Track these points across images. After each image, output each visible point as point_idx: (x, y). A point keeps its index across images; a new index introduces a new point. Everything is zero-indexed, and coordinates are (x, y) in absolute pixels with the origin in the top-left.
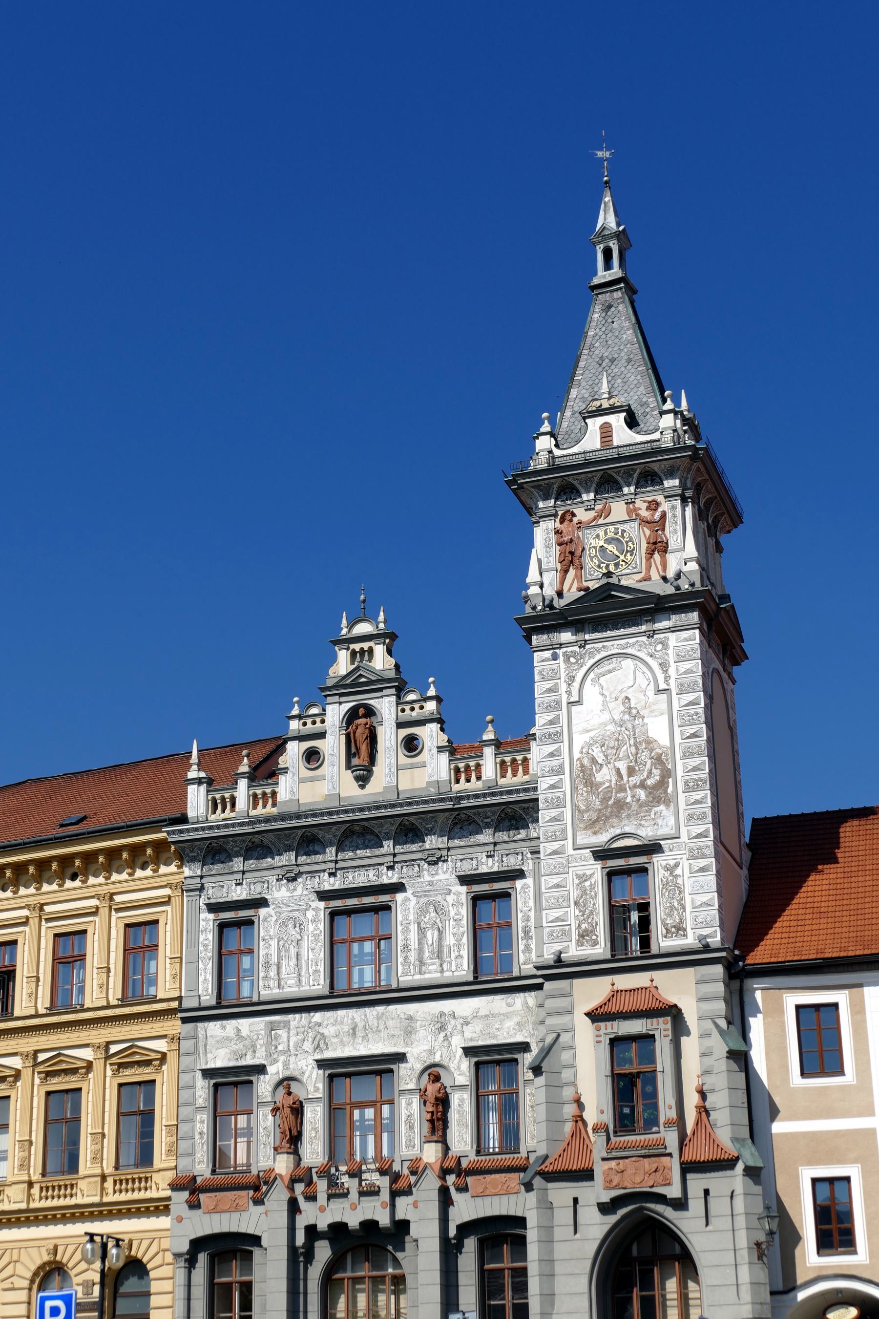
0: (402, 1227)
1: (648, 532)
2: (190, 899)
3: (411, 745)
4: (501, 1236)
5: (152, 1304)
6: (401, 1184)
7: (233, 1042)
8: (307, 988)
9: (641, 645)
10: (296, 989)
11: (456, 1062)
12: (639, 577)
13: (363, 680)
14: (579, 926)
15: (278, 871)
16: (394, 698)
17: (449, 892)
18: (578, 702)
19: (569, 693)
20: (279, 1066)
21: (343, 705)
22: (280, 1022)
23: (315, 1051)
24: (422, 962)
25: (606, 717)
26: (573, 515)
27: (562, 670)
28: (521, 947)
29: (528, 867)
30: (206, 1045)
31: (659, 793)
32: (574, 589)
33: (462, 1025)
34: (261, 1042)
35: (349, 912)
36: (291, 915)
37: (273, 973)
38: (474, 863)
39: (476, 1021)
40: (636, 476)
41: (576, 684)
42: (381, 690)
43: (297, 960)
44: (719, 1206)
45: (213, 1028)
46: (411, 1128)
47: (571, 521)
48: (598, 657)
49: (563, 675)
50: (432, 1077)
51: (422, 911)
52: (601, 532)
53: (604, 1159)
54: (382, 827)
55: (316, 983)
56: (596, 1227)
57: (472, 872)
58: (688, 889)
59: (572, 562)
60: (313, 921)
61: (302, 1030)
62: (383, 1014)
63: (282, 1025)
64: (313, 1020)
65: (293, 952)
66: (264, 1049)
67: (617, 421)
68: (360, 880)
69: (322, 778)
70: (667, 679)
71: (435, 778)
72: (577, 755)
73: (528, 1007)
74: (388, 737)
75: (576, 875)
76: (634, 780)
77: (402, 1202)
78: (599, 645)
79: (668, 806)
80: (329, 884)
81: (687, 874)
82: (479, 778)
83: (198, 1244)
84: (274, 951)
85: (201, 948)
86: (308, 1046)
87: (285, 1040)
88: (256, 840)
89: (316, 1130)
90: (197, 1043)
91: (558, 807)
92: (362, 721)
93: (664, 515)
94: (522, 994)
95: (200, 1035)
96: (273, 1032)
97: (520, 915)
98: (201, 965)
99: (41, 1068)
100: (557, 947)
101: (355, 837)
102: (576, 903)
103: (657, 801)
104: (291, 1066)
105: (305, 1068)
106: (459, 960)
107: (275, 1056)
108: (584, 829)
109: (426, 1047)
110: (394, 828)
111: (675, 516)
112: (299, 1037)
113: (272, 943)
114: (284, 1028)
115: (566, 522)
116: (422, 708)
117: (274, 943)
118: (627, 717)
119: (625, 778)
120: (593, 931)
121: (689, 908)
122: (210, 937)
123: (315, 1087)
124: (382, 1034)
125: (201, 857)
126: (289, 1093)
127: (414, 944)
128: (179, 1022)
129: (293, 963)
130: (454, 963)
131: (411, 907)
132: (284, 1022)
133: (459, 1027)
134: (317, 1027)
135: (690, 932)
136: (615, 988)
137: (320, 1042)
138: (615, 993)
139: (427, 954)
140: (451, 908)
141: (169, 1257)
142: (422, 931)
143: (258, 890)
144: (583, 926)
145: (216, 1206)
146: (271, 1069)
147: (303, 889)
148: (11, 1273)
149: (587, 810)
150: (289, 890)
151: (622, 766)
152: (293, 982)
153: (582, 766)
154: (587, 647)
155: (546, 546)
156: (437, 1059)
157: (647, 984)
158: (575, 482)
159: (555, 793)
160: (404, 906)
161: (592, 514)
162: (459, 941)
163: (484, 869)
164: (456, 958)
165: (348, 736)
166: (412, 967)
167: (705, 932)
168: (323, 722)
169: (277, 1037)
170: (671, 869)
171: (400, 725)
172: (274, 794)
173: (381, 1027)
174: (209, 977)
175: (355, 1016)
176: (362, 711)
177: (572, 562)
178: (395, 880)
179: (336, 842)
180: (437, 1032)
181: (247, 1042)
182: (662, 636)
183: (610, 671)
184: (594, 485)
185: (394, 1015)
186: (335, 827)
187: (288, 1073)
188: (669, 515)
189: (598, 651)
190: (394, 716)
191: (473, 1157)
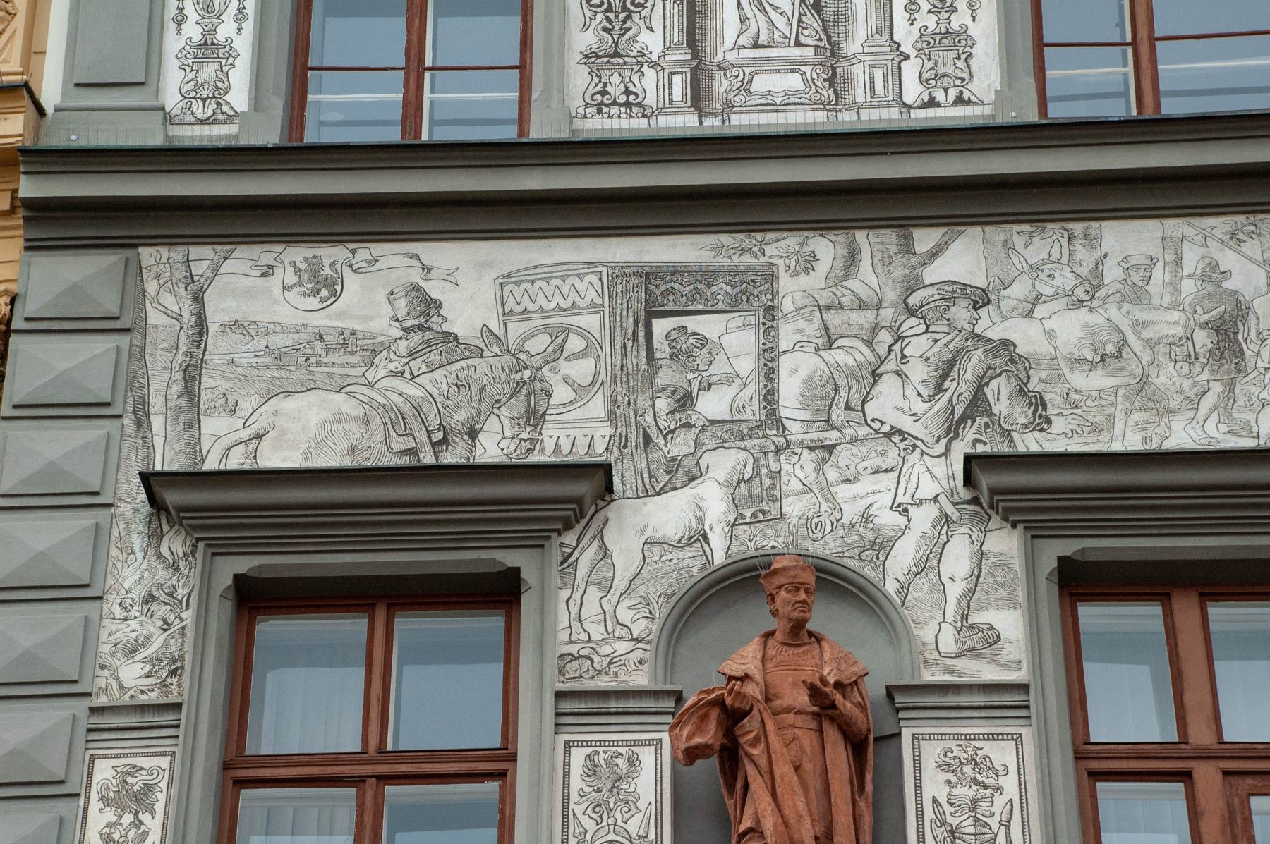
20: (710, 500)
22: (709, 276)
23: (953, 430)
30: (191, 373)
34: (582, 370)
45: (256, 289)
61: (863, 319)
63: (722, 288)
64: (933, 274)
66: (597, 406)
87: (746, 365)
95: (154, 317)
96: (661, 327)
104: (794, 508)
105: (887, 519)
107: (680, 446)
112: (837, 356)
114: (733, 306)
123: (964, 623)
126: (799, 633)
132: (735, 275)
134: (961, 313)
152: (794, 82)
175: (1228, 259)
181: (480, 370)
187: (768, 539)
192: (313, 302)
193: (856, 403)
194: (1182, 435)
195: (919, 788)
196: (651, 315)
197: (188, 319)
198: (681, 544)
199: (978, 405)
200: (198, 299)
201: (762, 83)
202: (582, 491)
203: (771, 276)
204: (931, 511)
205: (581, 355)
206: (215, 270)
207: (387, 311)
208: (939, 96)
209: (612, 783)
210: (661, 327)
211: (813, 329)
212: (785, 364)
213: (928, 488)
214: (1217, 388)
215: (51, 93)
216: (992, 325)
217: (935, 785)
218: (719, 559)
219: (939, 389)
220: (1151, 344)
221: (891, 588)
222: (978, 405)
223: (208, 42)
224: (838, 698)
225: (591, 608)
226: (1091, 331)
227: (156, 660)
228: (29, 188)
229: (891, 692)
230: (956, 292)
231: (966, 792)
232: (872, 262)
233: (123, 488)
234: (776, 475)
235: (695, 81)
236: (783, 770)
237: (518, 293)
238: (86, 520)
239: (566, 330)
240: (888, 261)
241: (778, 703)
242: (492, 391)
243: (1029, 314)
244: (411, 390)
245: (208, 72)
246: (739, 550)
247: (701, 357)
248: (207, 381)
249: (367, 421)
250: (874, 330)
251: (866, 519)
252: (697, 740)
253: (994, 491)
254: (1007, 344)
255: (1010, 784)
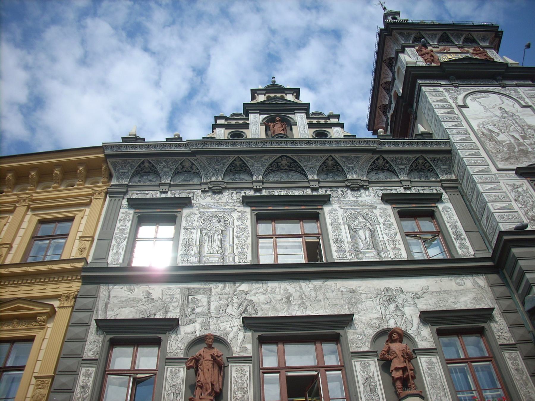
2: (113, 199)
7: (140, 303)
11: (414, 328)
14: (526, 214)
17: (375, 208)
18: (465, 106)
22: (199, 289)
29: (445, 196)
30: (106, 304)
33: (413, 298)
34: (176, 304)
36: (215, 214)
39: (427, 296)
43: (221, 244)
48: (469, 92)
50: (396, 336)
54: (309, 161)
61: (226, 296)
62: (321, 287)
63: (202, 291)
64: (239, 289)
65: (217, 238)
66: (178, 310)
72: (476, 128)
73: (480, 286)
75: (508, 184)
87: (205, 304)
88: (187, 164)
95: (101, 295)
96: (190, 297)
97: (448, 225)
98: (114, 242)
101: (279, 173)
102: (515, 200)
104: (212, 327)
105: (229, 329)
106: (397, 251)
107: (192, 317)
108: (501, 161)
109: (376, 316)
110: (319, 164)
113: (195, 231)
114: (203, 294)
118: (506, 115)
122: (129, 224)
123: (241, 347)
124: (322, 303)
125: (130, 174)
129: (216, 245)
133: (410, 300)
134: (243, 295)
140: (379, 218)
149: (499, 152)
152: (217, 259)
153: (483, 133)
156: (391, 324)
164: (393, 249)
166: (347, 254)
173: (320, 297)
179: (263, 171)
180: (386, 303)
186: (266, 156)
187: (206, 333)
189: (469, 90)
192: (129, 293)
193: (224, 310)
194: (280, 314)
195: (231, 375)
196: (189, 295)
197: (107, 295)
198: (191, 333)
199: (246, 310)
200: (109, 292)
201: (210, 259)
203: (210, 289)
204: (237, 328)
205: (176, 302)
206: (113, 288)
207: (142, 294)
208: (241, 261)
209: (175, 374)
210: (190, 297)
211: (217, 298)
212: (212, 304)
213: (236, 324)
214: (287, 307)
215: (89, 260)
216: (249, 297)
217: (234, 374)
218: (198, 336)
219: (239, 308)
220: (276, 301)
221: (228, 341)
222: (246, 310)
223: (117, 253)
224: (217, 358)
225: (174, 344)
226: (266, 298)
227: (94, 352)
228: (83, 274)
229: (227, 358)
230: (243, 292)
231: (240, 375)
232: (229, 287)
233: (92, 323)
234: (209, 322)
235: (199, 259)
236: (205, 370)
237: (165, 291)
238: (85, 328)
239: (173, 298)
240: (231, 287)
241: (205, 359)
242: (159, 308)
243: (255, 296)
244: (145, 307)
245: (116, 257)
246: (201, 335)
247: (197, 302)
248: (109, 306)
249: (136, 313)
250: (228, 298)
251: (225, 329)
252: (190, 365)
253: (248, 324)
254: (251, 300)
255: (248, 374)
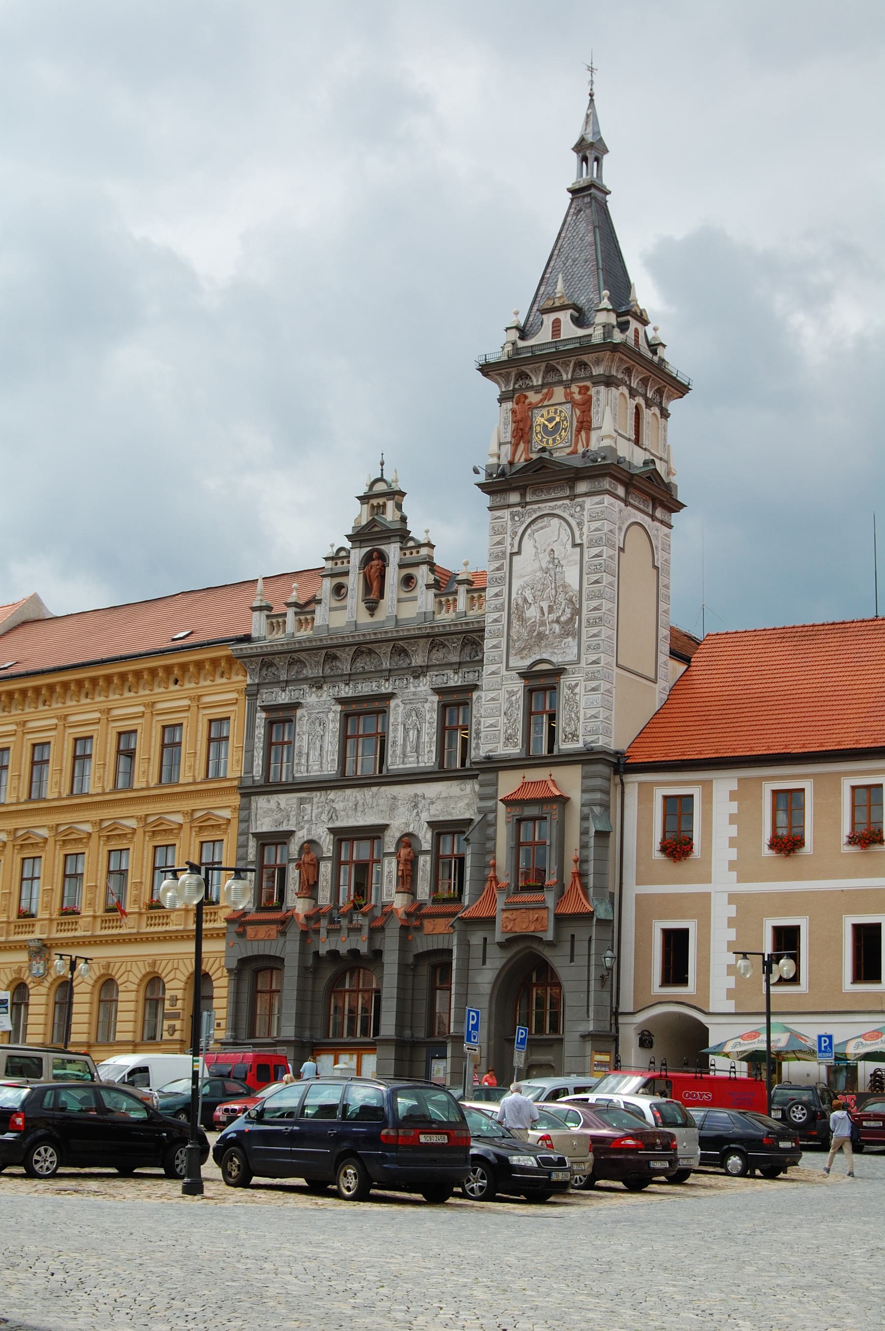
0: (377, 954)
1: (578, 412)
3: (408, 581)
4: (438, 964)
5: (214, 1006)
6: (378, 924)
8: (326, 773)
9: (565, 507)
10: (319, 773)
12: (568, 450)
13: (376, 529)
15: (309, 682)
16: (398, 545)
18: (519, 553)
19: (512, 545)
20: (305, 831)
21: (362, 549)
24: (405, 755)
25: (536, 565)
26: (526, 397)
27: (509, 526)
28: (473, 745)
31: (570, 629)
32: (522, 460)
34: (293, 813)
35: (359, 714)
36: (318, 716)
37: (303, 761)
38: (445, 678)
39: (439, 801)
40: (572, 365)
41: (517, 538)
42: (389, 537)
44: (581, 948)
45: (261, 803)
46: (390, 881)
47: (524, 403)
48: (534, 516)
49: (509, 530)
51: (408, 716)
52: (544, 411)
53: (503, 910)
55: (330, 769)
56: (496, 961)
57: (444, 686)
58: (582, 705)
59: (522, 436)
60: (332, 721)
67: (565, 317)
68: (366, 690)
69: (344, 608)
70: (581, 535)
71: (423, 610)
72: (514, 596)
74: (393, 575)
76: (553, 617)
77: (378, 937)
78: (535, 506)
79: (574, 638)
80: (346, 691)
81: (583, 693)
82: (454, 611)
83: (244, 962)
84: (305, 744)
85: (256, 740)
86: (324, 817)
89: (326, 880)
90: (250, 813)
91: (498, 636)
92: (375, 562)
93: (591, 397)
94: (471, 781)
97: (474, 720)
98: (255, 754)
99: (149, 829)
100: (490, 747)
103: (566, 634)
104: (313, 832)
109: (404, 821)
110: (389, 650)
111: (598, 400)
115: (520, 404)
116: (418, 552)
117: (305, 737)
118: (551, 566)
119: (546, 614)
120: (516, 735)
121: (582, 720)
125: (258, 669)
127: (400, 741)
128: (239, 797)
129: (317, 753)
130: (426, 757)
131: (400, 712)
132: (309, 798)
135: (581, 738)
136: (526, 780)
137: (333, 814)
138: (525, 784)
139: (408, 749)
141: (225, 973)
142: (406, 731)
143: (297, 696)
144: (509, 731)
145: (256, 935)
146: (299, 834)
147: (327, 695)
148: (126, 979)
150: (317, 696)
151: (545, 605)
153: (517, 605)
154: (528, 507)
155: (505, 424)
156: (411, 830)
157: (547, 778)
158: (528, 371)
159: (497, 626)
160: (397, 710)
161: (539, 397)
162: (431, 739)
163: (452, 683)
164: (429, 752)
165: (365, 574)
167: (589, 739)
168: (349, 562)
169: (304, 809)
170: (572, 688)
171: (401, 566)
172: (313, 619)
173: (374, 805)
174: (260, 763)
176: (375, 555)
177: (522, 436)
178: (390, 690)
179: (350, 660)
181: (284, 813)
182: (580, 500)
183: (542, 528)
184: (541, 373)
185: (384, 795)
186: (348, 648)
187: (310, 837)
188: (594, 399)
190: (397, 560)
191: (429, 904)
202: (291, 833)
